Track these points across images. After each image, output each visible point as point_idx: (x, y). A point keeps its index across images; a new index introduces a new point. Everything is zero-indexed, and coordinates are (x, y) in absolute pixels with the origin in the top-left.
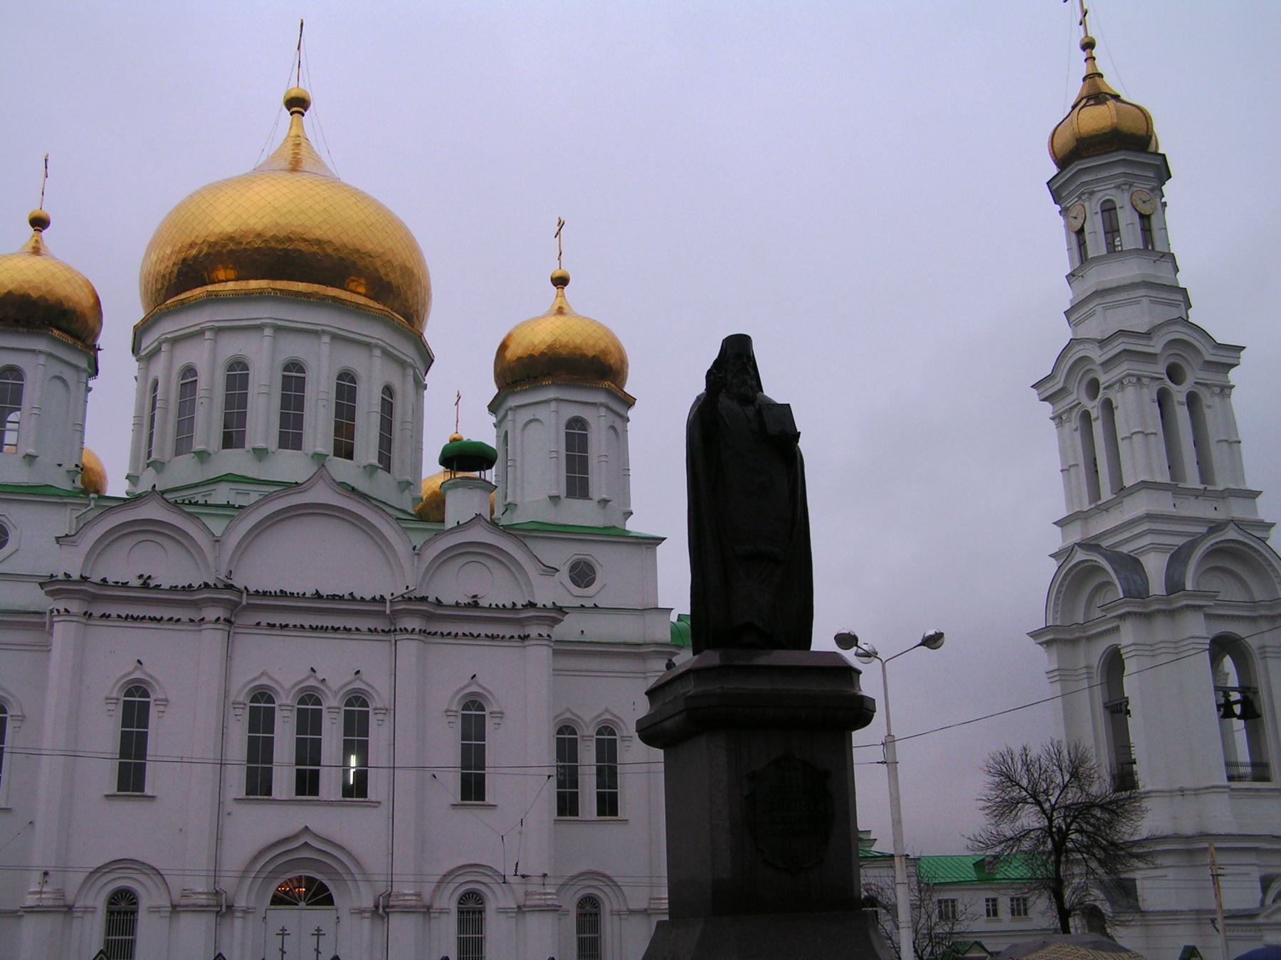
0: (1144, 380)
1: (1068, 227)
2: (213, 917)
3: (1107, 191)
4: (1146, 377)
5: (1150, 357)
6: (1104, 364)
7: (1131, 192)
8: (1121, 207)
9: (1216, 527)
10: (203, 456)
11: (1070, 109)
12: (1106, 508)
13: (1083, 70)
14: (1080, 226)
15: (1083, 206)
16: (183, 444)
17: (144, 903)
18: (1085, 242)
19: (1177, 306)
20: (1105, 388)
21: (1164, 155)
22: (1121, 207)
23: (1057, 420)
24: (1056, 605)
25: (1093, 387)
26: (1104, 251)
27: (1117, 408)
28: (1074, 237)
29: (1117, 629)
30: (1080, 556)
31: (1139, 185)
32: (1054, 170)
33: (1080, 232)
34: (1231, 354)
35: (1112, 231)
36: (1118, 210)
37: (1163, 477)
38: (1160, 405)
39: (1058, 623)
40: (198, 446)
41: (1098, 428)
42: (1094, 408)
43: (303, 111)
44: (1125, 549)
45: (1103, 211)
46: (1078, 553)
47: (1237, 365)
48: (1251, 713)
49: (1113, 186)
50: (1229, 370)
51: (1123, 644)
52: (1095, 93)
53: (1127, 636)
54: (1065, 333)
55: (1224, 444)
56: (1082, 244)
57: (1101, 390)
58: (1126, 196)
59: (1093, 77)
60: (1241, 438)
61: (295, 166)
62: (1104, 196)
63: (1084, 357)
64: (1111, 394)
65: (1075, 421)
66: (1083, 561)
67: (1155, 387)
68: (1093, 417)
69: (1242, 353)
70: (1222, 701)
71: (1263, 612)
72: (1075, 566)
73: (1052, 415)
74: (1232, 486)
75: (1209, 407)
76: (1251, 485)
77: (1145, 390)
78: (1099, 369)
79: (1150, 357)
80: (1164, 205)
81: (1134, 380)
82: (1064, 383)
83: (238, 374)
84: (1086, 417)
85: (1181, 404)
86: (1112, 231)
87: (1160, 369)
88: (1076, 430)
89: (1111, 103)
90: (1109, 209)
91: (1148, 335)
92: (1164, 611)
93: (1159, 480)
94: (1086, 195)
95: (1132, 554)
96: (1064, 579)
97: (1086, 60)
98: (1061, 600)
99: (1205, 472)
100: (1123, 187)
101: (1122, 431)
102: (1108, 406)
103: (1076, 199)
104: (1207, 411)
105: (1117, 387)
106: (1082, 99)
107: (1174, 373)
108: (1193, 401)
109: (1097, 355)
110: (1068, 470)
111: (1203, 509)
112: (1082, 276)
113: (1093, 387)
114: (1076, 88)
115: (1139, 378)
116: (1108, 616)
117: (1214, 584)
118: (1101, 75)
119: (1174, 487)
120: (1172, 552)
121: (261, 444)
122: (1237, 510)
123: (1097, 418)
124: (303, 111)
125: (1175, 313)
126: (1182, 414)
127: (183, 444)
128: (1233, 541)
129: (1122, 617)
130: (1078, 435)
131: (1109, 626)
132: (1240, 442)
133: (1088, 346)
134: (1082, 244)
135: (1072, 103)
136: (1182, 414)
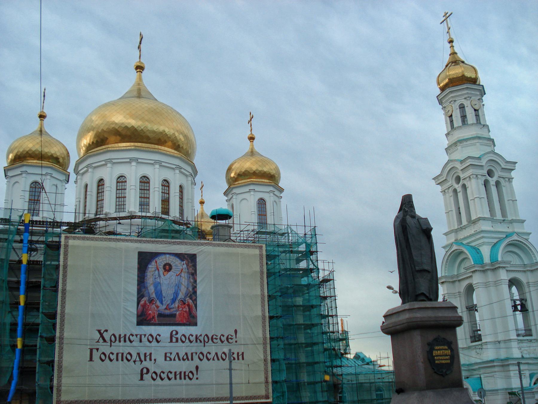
0: (479, 176)
1: (446, 114)
4: (479, 175)
6: (462, 170)
7: (470, 100)
8: (467, 107)
11: (444, 67)
12: (464, 228)
13: (449, 51)
14: (451, 114)
15: (452, 106)
18: (453, 121)
19: (490, 146)
20: (463, 180)
21: (483, 86)
22: (467, 107)
23: (443, 192)
24: (445, 267)
25: (458, 179)
26: (460, 124)
27: (468, 187)
28: (448, 119)
29: (471, 276)
30: (455, 247)
31: (473, 98)
32: (439, 92)
33: (451, 116)
34: (513, 165)
35: (464, 117)
36: (466, 108)
37: (488, 215)
38: (485, 186)
39: (447, 274)
41: (460, 196)
42: (458, 187)
43: (141, 71)
44: (473, 244)
45: (460, 108)
46: (454, 246)
47: (513, 170)
48: (524, 309)
49: (464, 98)
51: (474, 283)
52: (455, 61)
53: (476, 279)
54: (446, 158)
55: (511, 201)
56: (452, 122)
57: (461, 181)
58: (469, 102)
59: (454, 54)
60: (517, 199)
61: (139, 96)
62: (460, 102)
63: (454, 167)
64: (465, 182)
65: (451, 193)
66: (456, 250)
67: (484, 178)
68: (458, 191)
69: (516, 165)
70: (513, 304)
71: (529, 269)
72: (453, 251)
73: (441, 191)
74: (514, 218)
75: (504, 186)
76: (521, 217)
77: (479, 180)
78: (461, 172)
80: (483, 105)
81: (475, 176)
82: (446, 177)
83: (121, 180)
84: (455, 191)
85: (493, 185)
86: (464, 117)
87: (485, 172)
88: (451, 196)
89: (461, 64)
91: (479, 158)
92: (490, 269)
93: (486, 216)
94: (453, 102)
95: (476, 246)
96: (449, 257)
97: (450, 47)
99: (504, 213)
100: (468, 98)
101: (470, 197)
102: (464, 187)
103: (449, 103)
104: (504, 188)
105: (468, 179)
106: (449, 63)
107: (490, 173)
108: (498, 184)
109: (459, 167)
110: (448, 212)
111: (503, 228)
112: (452, 134)
113: (458, 179)
114: (447, 58)
116: (468, 272)
117: (510, 258)
118: (456, 53)
119: (492, 219)
120: (492, 245)
122: (517, 228)
123: (460, 192)
124: (141, 71)
125: (489, 149)
126: (494, 189)
128: (516, 240)
129: (474, 272)
130: (452, 198)
131: (469, 275)
132: (516, 200)
133: (456, 163)
134: (452, 122)
135: (445, 64)
136: (494, 189)
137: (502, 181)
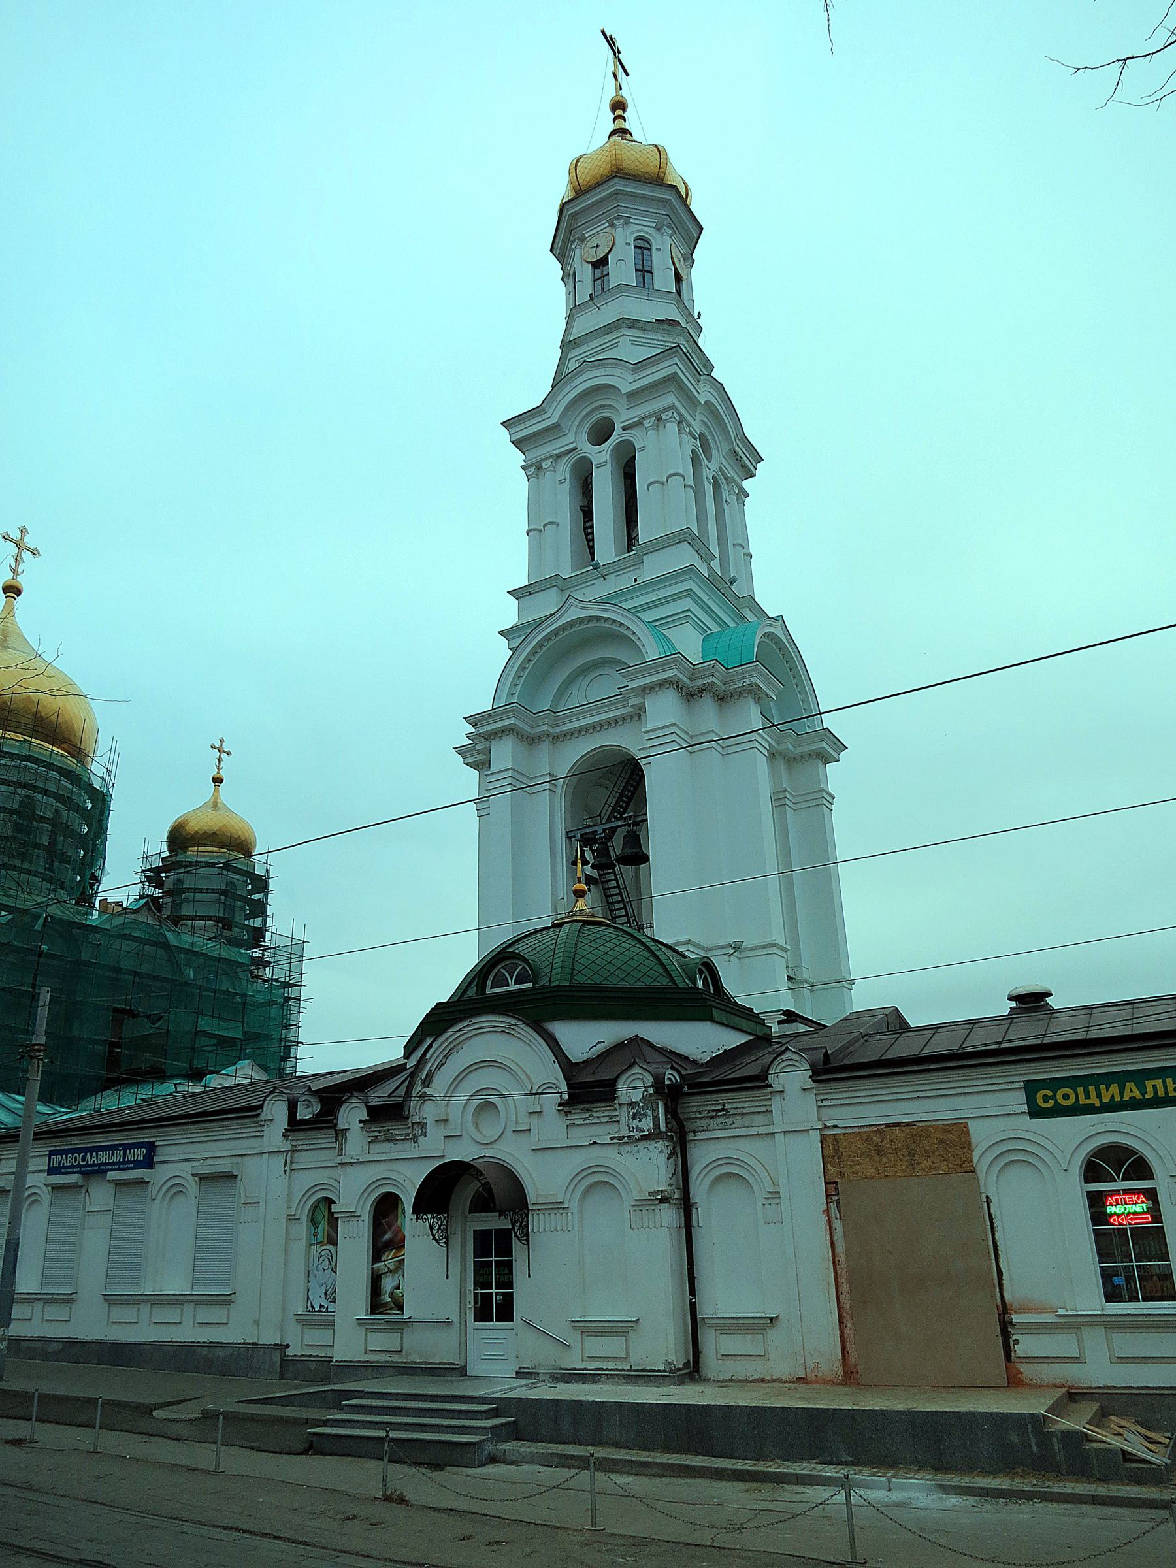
3: (645, 228)
6: (631, 395)
25: (601, 432)
42: (601, 456)
45: (635, 247)
62: (642, 230)
72: (563, 628)
86: (644, 271)
90: (643, 246)
94: (621, 222)
98: (522, 679)
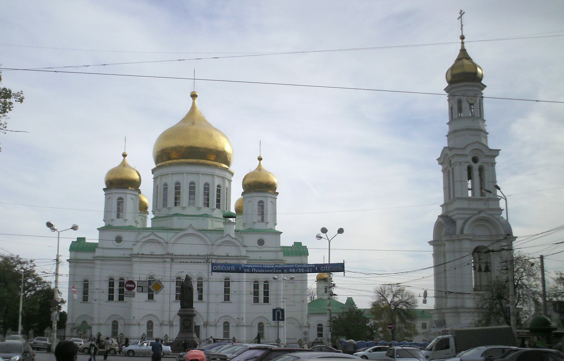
0: (462, 163)
2: (169, 327)
5: (465, 155)
9: (480, 212)
10: (169, 208)
16: (165, 205)
17: (155, 323)
40: (169, 206)
42: (450, 169)
47: (496, 156)
50: (495, 157)
67: (467, 165)
79: (465, 155)
81: (458, 163)
87: (469, 159)
91: (464, 148)
102: (453, 169)
107: (475, 160)
115: (460, 163)
121: (184, 206)
127: (165, 205)
137: (485, 166)
